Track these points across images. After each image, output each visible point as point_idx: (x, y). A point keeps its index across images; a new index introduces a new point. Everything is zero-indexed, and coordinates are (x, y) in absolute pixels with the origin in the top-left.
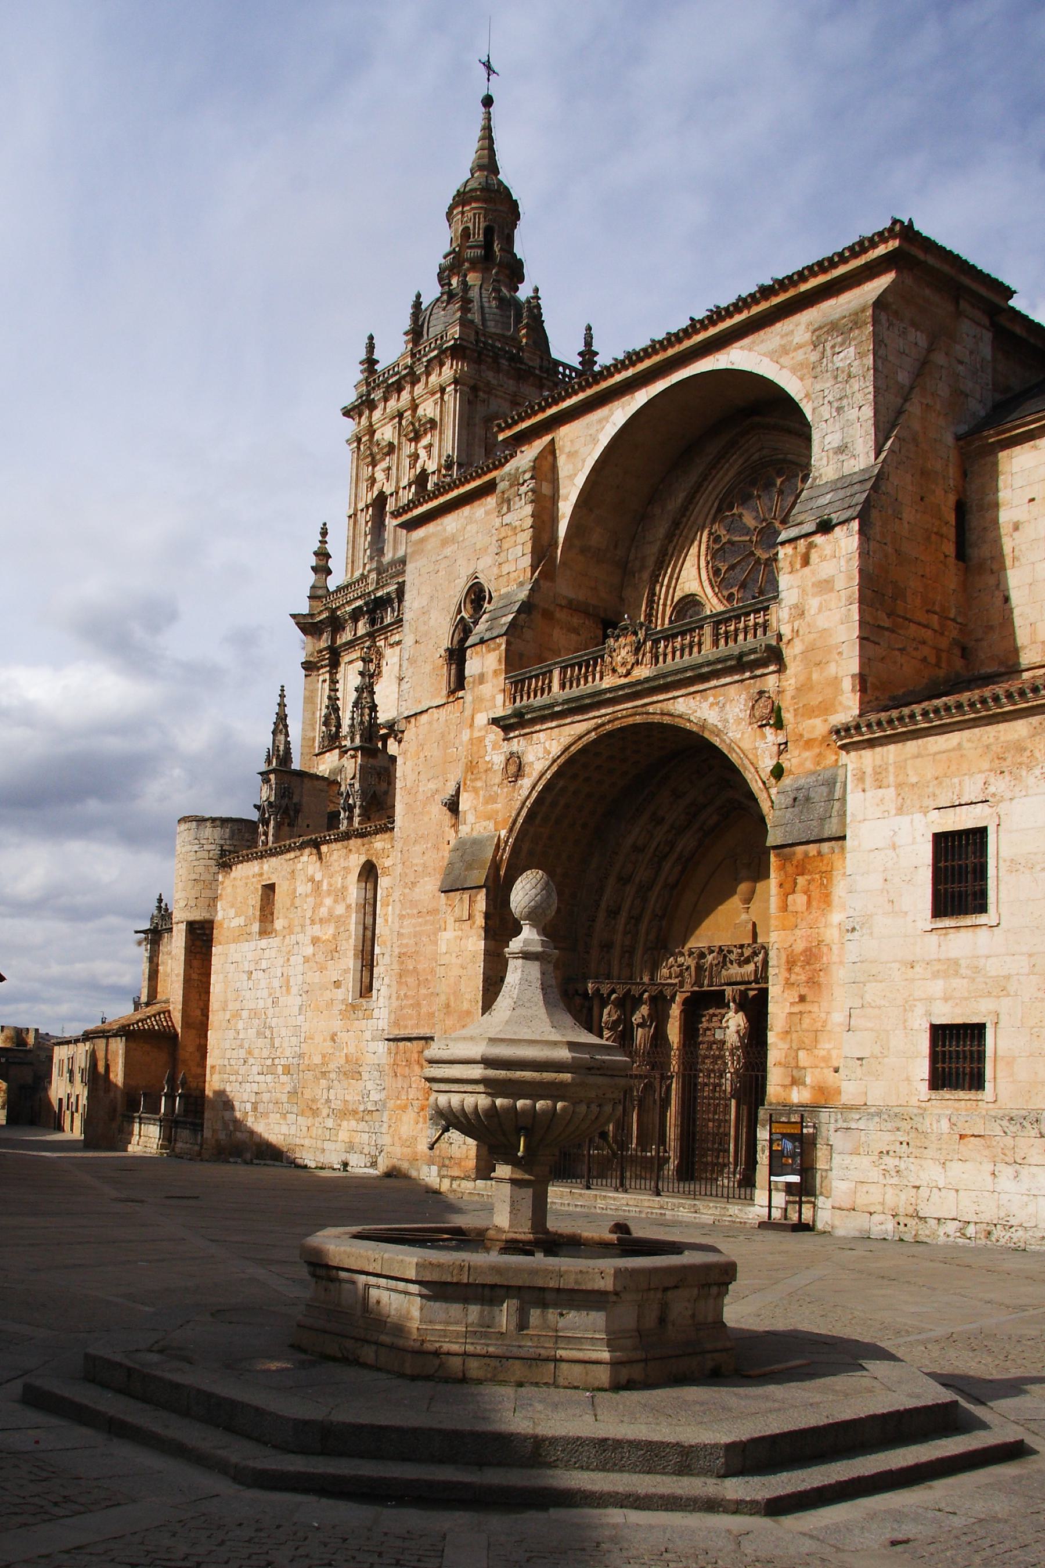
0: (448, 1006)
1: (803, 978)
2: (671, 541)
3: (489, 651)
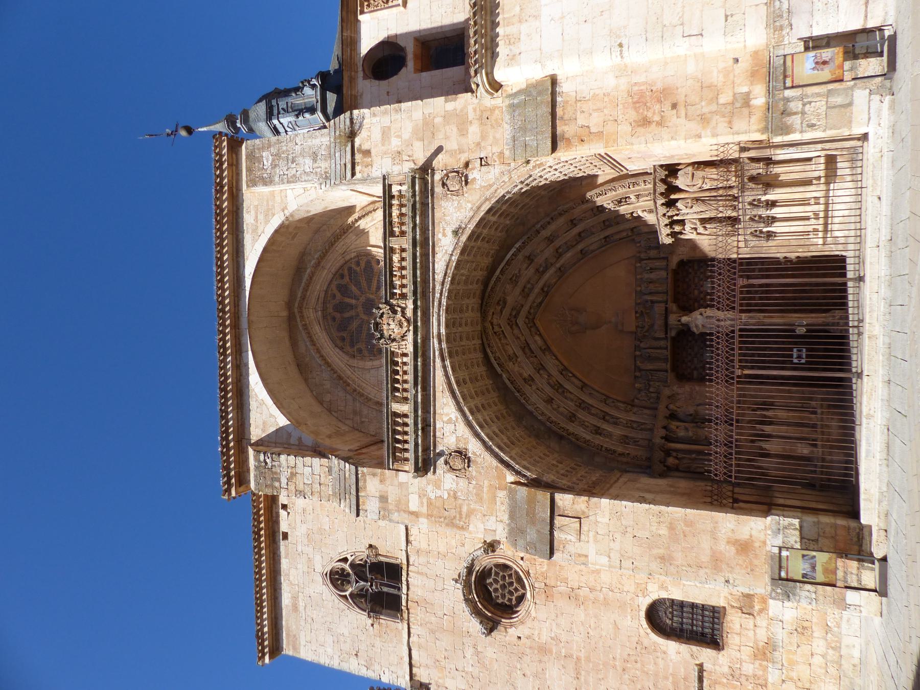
0: (662, 558)
2: (348, 385)
3: (365, 487)
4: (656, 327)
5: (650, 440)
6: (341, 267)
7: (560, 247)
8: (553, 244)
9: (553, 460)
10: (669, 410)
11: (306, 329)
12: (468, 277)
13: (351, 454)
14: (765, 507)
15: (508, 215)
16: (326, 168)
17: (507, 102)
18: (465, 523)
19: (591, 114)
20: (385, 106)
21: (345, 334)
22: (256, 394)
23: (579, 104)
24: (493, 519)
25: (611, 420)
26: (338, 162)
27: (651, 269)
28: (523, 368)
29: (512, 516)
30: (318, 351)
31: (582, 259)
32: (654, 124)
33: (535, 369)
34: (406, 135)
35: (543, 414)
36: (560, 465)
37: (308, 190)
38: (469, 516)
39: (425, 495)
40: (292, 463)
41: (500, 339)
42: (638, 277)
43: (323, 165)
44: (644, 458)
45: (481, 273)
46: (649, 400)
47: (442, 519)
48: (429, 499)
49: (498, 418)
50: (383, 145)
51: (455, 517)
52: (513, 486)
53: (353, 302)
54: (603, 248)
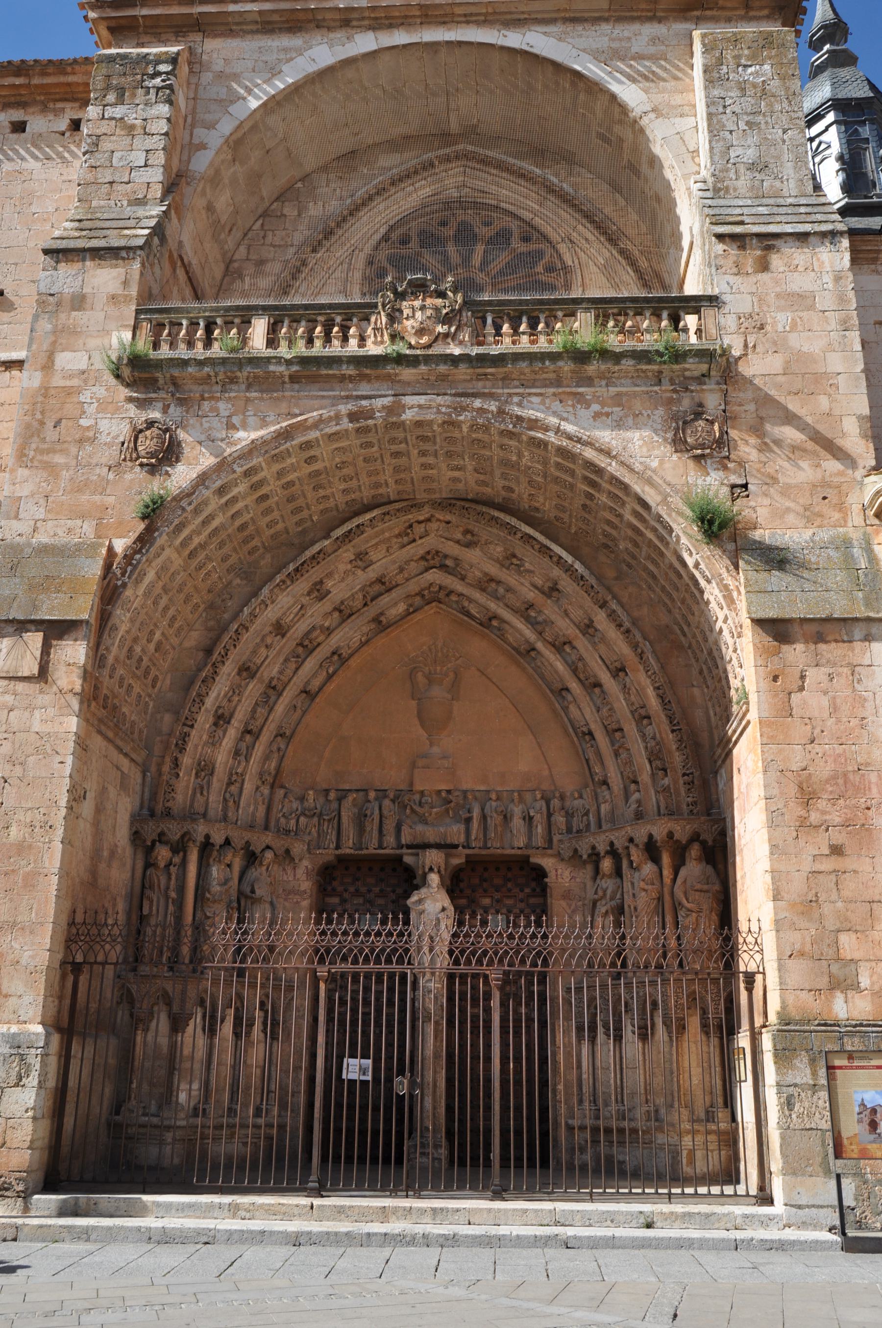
1: (836, 818)
2: (314, 251)
4: (420, 828)
5: (204, 815)
6: (545, 238)
7: (574, 648)
8: (580, 635)
9: (163, 634)
10: (263, 850)
11: (424, 168)
12: (515, 466)
13: (172, 244)
14: (65, 1023)
15: (636, 544)
16: (735, 190)
17: (855, 536)
18: (32, 460)
19: (825, 693)
20: (854, 300)
21: (414, 244)
22: (292, 59)
23: (846, 671)
24: (41, 514)
25: (243, 746)
26: (746, 211)
27: (531, 818)
28: (343, 580)
29: (44, 550)
30: (380, 191)
31: (552, 691)
32: (803, 813)
33: (342, 603)
34: (795, 341)
35: (253, 616)
36: (152, 647)
37: (693, 158)
38: (44, 468)
39: (85, 381)
40: (153, 127)
41: (399, 535)
42: (516, 794)
43: (743, 184)
44: (168, 804)
45: (525, 496)
46: (283, 816)
47: (38, 416)
48: (79, 391)
49: (243, 527)
50: (778, 296)
51: (44, 440)
52: (104, 551)
53: (477, 259)
54: (571, 730)
